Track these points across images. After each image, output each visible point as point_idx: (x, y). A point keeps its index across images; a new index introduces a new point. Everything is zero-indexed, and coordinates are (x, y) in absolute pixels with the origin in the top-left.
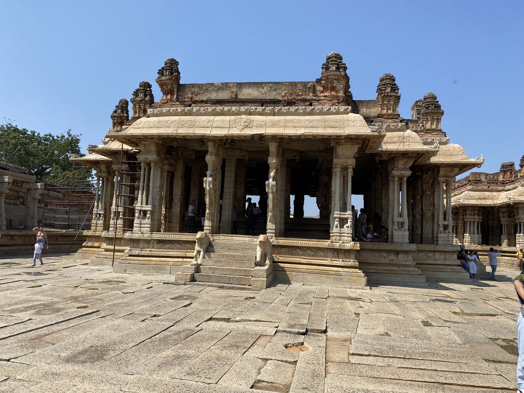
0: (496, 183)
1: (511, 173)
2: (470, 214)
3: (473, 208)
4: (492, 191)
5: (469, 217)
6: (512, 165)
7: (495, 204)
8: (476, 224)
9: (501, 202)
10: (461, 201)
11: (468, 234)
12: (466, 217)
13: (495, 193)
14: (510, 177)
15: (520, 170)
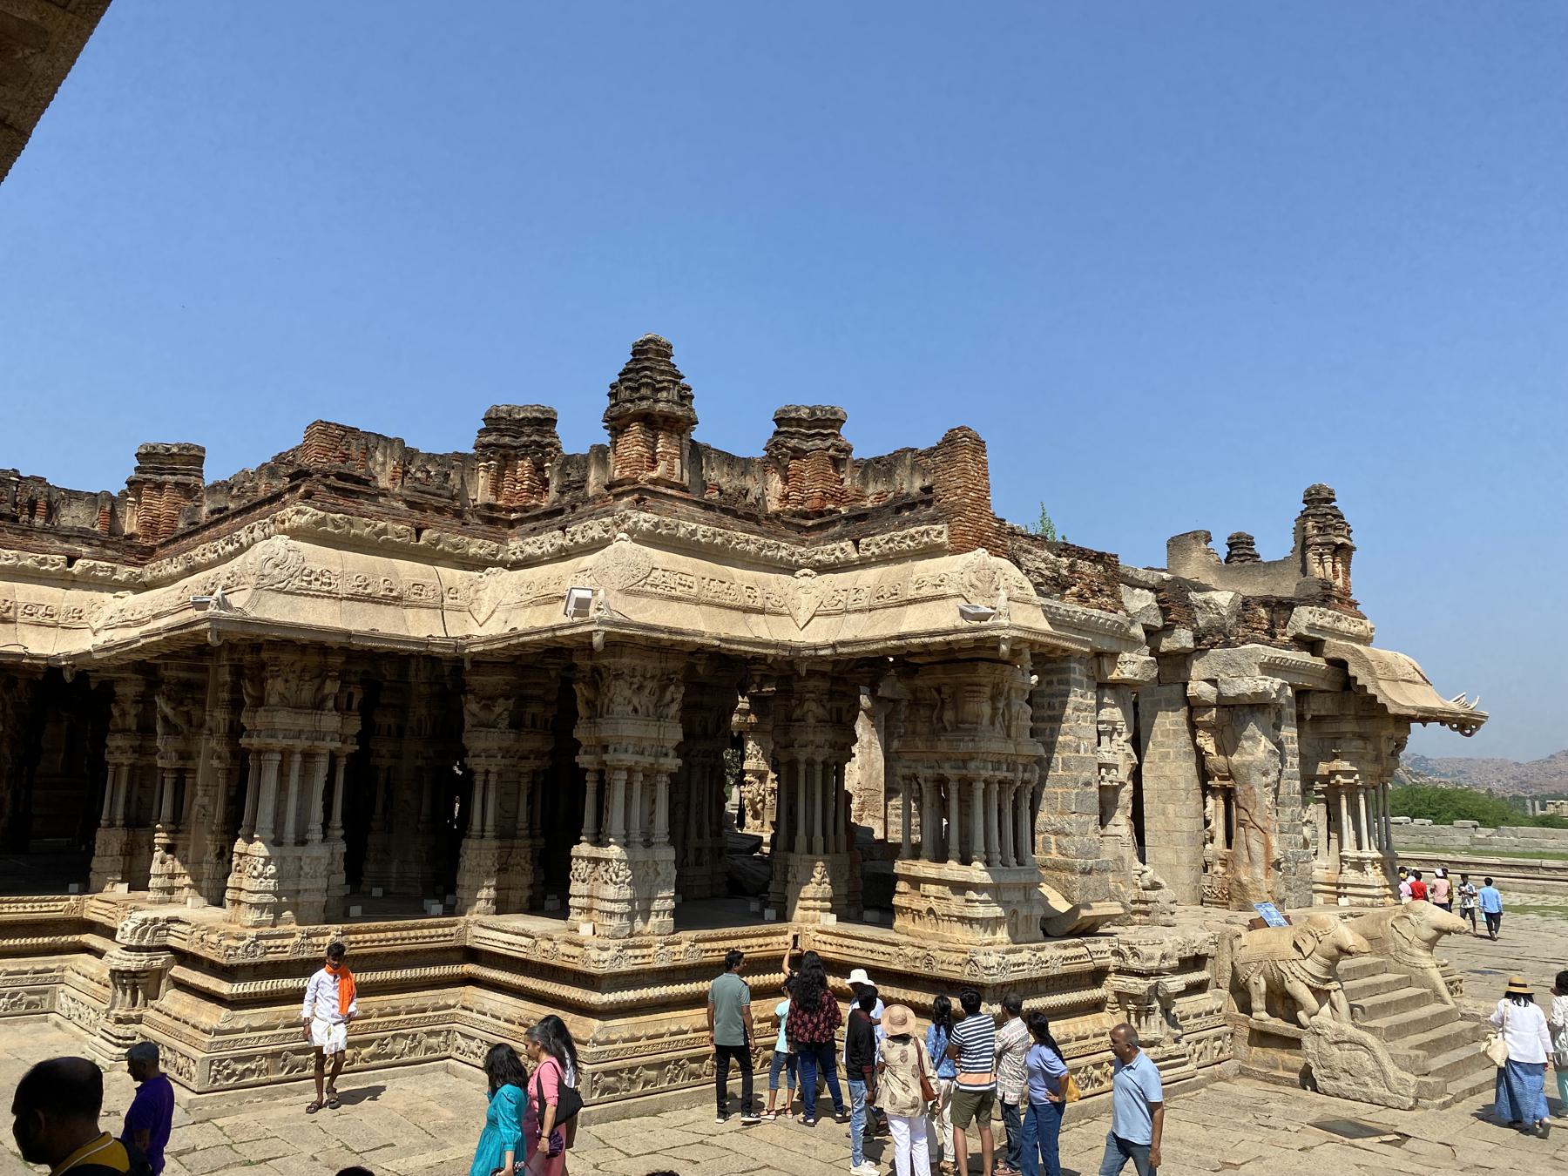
0: (458, 514)
1: (539, 468)
2: (285, 703)
3: (313, 660)
4: (430, 556)
5: (283, 719)
6: (545, 422)
7: (458, 645)
8: (322, 767)
9: (495, 628)
10: (237, 600)
11: (259, 848)
12: (261, 719)
13: (452, 575)
14: (531, 490)
15: (600, 453)
